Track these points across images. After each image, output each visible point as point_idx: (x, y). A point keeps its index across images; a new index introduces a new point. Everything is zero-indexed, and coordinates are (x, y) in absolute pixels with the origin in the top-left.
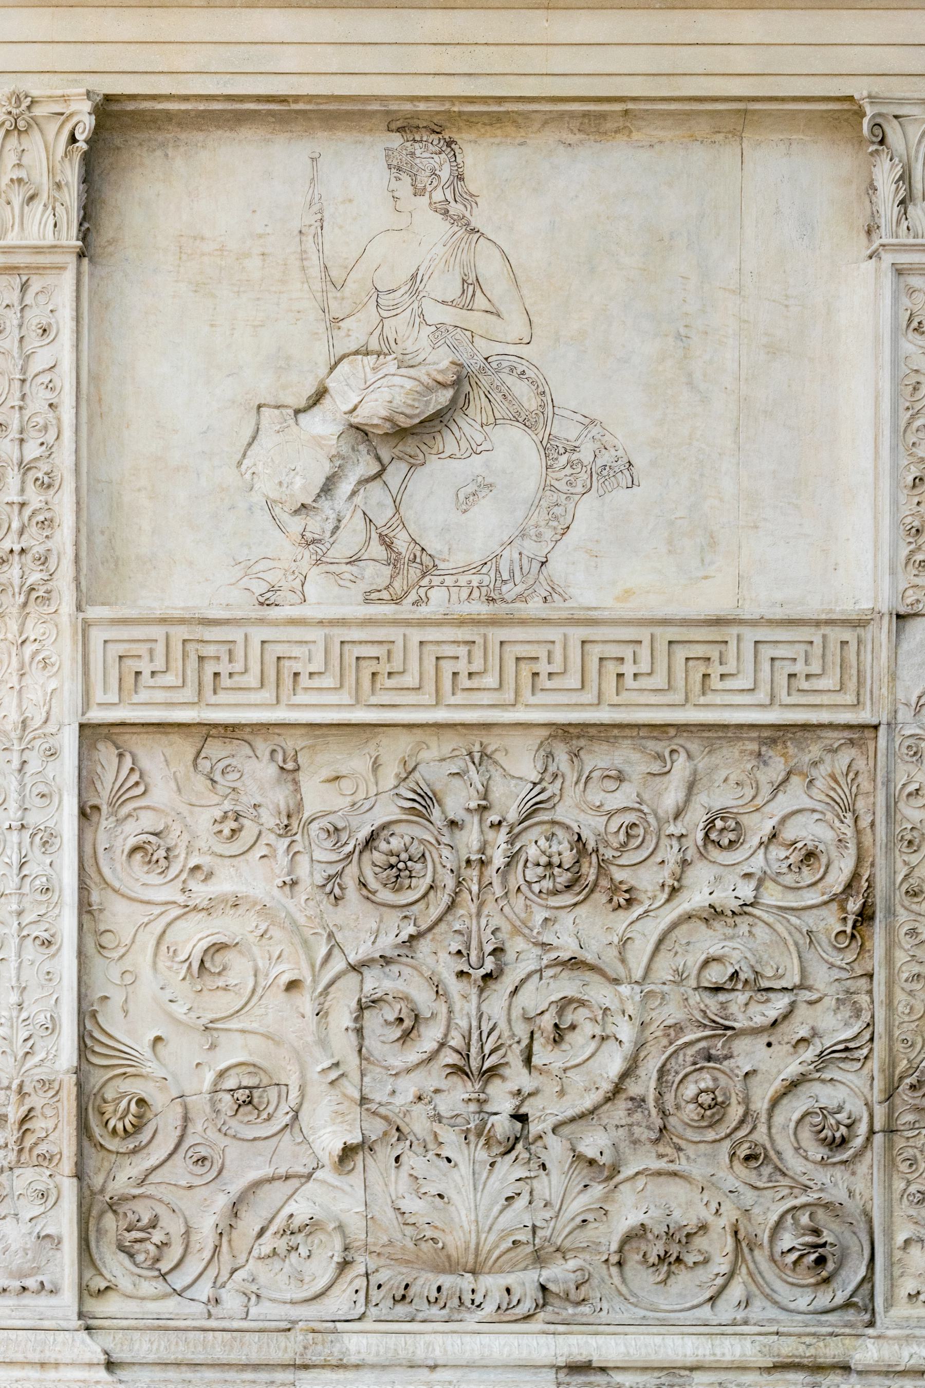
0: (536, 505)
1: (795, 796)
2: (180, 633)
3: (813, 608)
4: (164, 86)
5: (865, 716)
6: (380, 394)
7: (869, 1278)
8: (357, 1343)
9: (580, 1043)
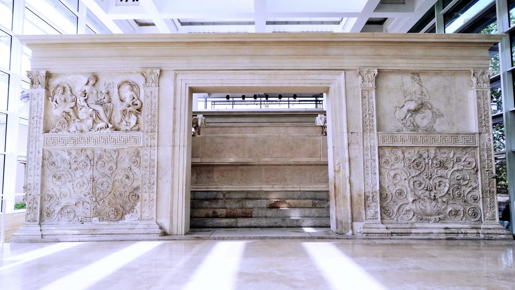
0: (431, 119)
1: (467, 156)
2: (390, 135)
3: (467, 132)
4: (385, 68)
5: (476, 145)
6: (412, 106)
7: (481, 217)
8: (417, 225)
9: (442, 187)
